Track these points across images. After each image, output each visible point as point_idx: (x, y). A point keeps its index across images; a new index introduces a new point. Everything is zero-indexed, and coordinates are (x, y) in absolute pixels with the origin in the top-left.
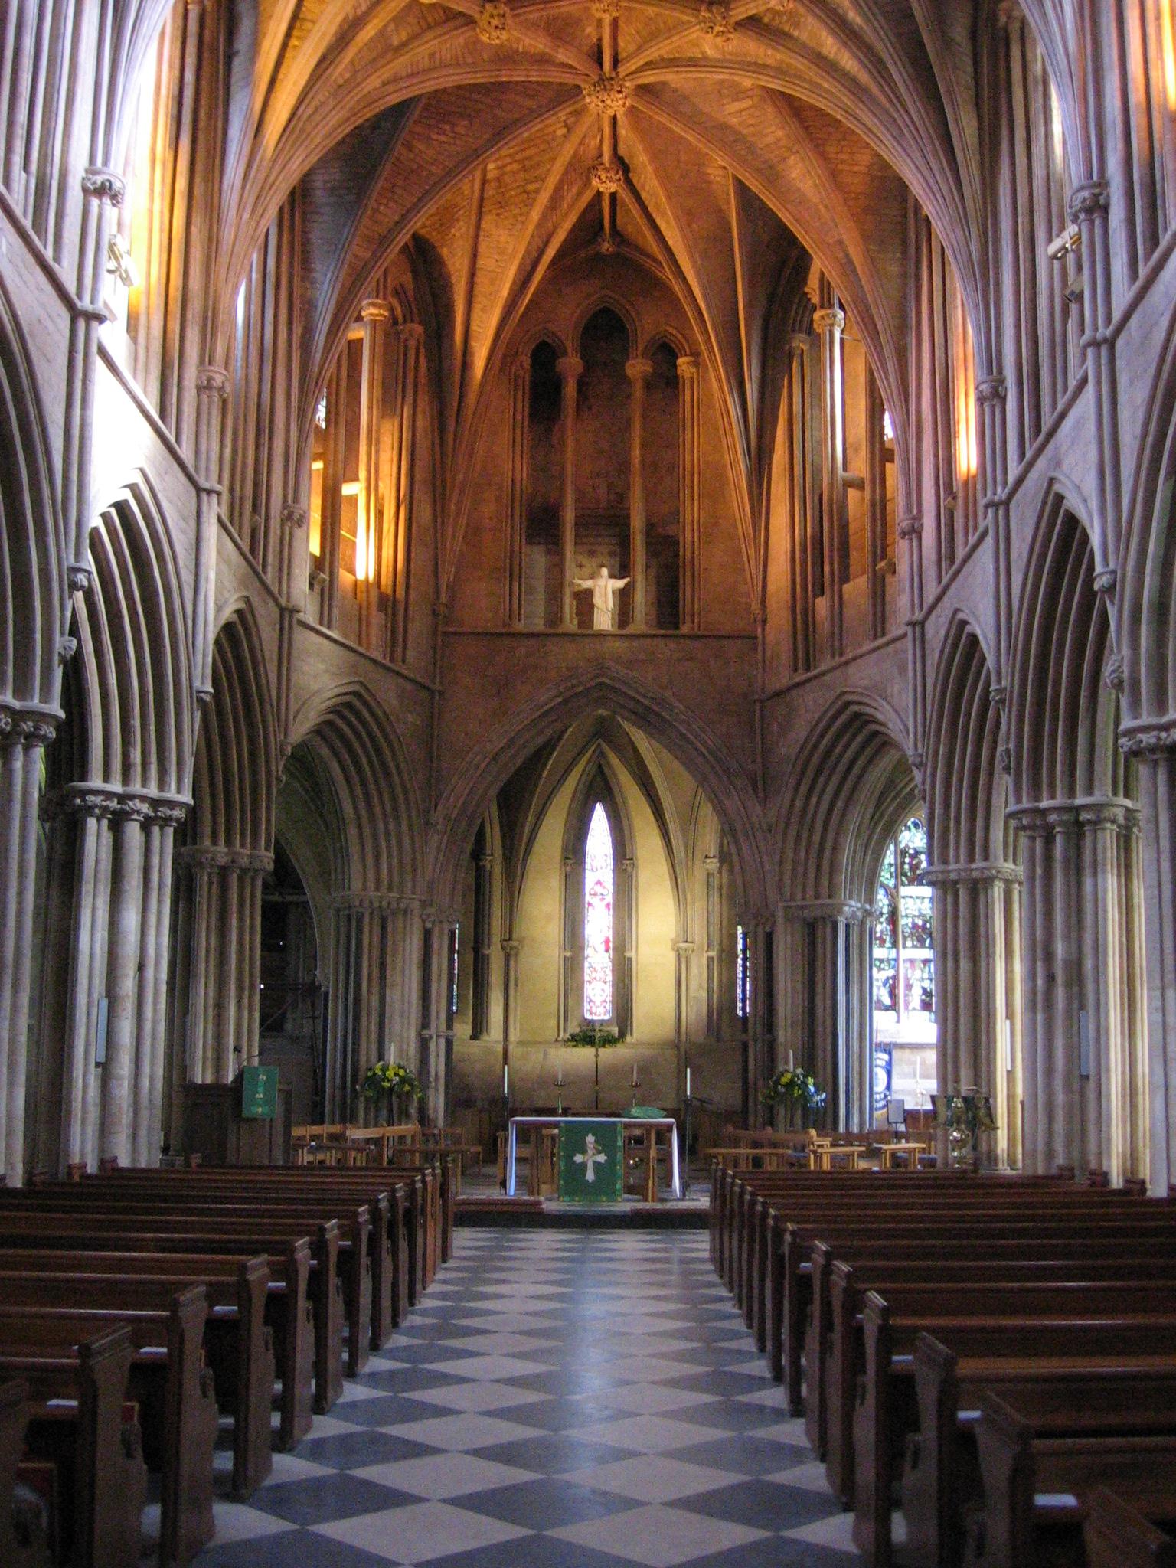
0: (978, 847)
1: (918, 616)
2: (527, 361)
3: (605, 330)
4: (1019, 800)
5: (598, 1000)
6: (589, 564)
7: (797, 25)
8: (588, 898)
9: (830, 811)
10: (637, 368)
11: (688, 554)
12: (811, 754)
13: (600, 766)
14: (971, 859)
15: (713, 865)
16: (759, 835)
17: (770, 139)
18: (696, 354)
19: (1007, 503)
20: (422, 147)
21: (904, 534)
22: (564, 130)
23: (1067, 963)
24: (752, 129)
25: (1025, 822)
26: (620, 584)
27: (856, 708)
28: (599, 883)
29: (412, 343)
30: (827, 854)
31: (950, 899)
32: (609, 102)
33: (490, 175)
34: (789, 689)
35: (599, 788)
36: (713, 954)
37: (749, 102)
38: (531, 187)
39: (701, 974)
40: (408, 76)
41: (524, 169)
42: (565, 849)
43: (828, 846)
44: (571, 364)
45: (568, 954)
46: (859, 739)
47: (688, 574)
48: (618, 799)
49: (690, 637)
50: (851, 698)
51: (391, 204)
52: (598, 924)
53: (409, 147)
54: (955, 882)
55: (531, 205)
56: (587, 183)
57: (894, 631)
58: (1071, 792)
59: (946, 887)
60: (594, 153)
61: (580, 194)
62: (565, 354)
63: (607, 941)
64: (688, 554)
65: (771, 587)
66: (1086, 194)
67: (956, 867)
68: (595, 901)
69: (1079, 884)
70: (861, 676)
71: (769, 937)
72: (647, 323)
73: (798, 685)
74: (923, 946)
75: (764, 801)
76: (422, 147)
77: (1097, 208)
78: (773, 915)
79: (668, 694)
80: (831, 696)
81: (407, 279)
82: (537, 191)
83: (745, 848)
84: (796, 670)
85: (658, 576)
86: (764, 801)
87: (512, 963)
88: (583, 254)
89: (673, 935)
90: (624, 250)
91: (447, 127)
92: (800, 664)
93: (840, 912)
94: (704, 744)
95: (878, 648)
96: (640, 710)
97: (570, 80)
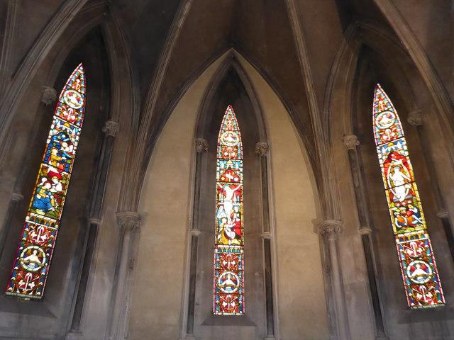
28: (229, 170)
35: (231, 92)
36: (367, 230)
39: (355, 256)
45: (197, 233)
52: (229, 208)
68: (227, 188)
87: (127, 238)
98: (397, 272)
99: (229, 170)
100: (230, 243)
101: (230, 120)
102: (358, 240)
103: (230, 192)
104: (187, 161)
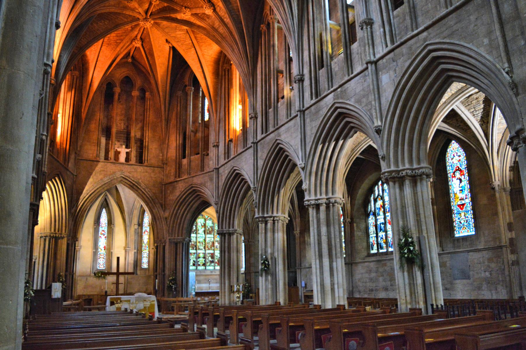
0: (231, 224)
1: (217, 167)
2: (105, 87)
3: (127, 81)
4: (259, 214)
5: (102, 263)
6: (118, 144)
7: (208, 18)
8: (100, 235)
9: (183, 215)
10: (135, 93)
11: (147, 144)
12: (180, 199)
13: (106, 199)
14: (229, 228)
15: (136, 227)
16: (162, 220)
17: (187, 43)
18: (152, 92)
19: (257, 143)
20: (95, 25)
21: (214, 146)
23: (271, 254)
25: (260, 219)
26: (128, 150)
27: (195, 188)
28: (103, 231)
29: (75, 77)
30: (182, 225)
31: (223, 238)
34: (174, 182)
37: (183, 32)
38: (118, 41)
41: (117, 36)
42: (95, 221)
43: (182, 222)
44: (117, 90)
46: (194, 196)
47: (146, 149)
48: (110, 207)
49: (146, 166)
50: (193, 186)
52: (102, 242)
53: (92, 24)
54: (225, 234)
56: (131, 43)
57: (207, 169)
58: (272, 213)
59: (221, 234)
60: (135, 36)
61: (129, 46)
62: (116, 86)
63: (105, 247)
64: (147, 144)
65: (169, 155)
66: (299, 77)
67: (225, 230)
68: (102, 236)
69: (273, 235)
70: (197, 180)
71: (164, 247)
72: (138, 82)
73: (176, 181)
74: (193, 249)
75: (164, 211)
76: (95, 25)
77: (301, 80)
78: (165, 241)
79: (140, 181)
80: (187, 185)
82: (120, 43)
83: (158, 222)
84: (176, 177)
85: (136, 149)
86: (164, 211)
88: (124, 60)
89: (124, 245)
92: (177, 176)
93: (184, 240)
94: (149, 195)
95: (203, 174)
96: (132, 184)
97: (137, 16)
98: (141, 260)
99: (103, 231)
100: (102, 252)
101: (104, 210)
102: (133, 253)
103: (103, 237)
104: (91, 230)
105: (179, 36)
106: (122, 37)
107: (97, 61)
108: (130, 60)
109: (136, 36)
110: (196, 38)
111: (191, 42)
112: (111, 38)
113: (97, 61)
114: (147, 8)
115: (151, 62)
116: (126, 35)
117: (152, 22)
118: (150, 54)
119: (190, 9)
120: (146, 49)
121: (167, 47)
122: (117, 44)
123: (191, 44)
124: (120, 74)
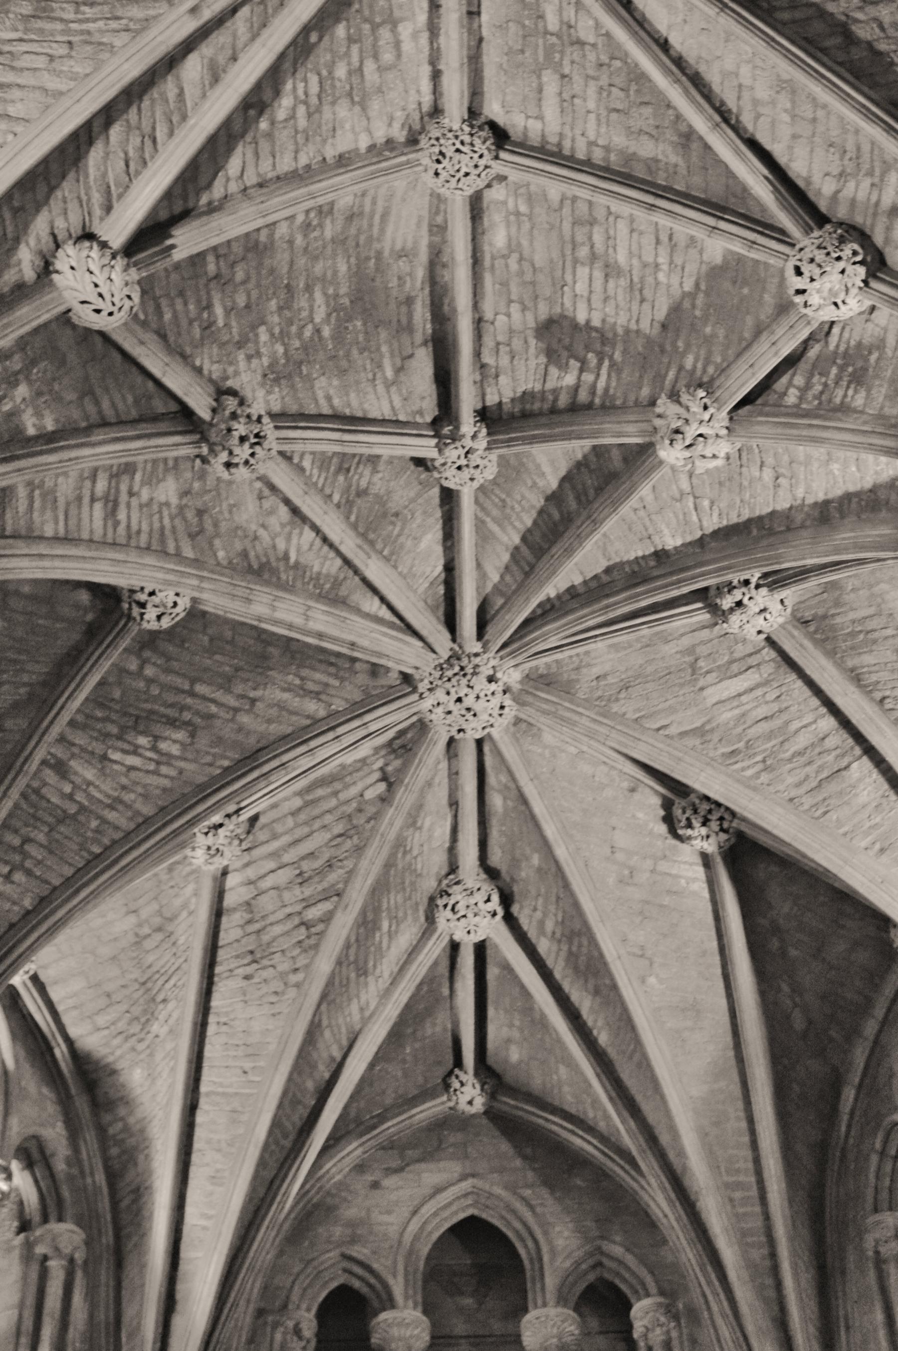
2: (309, 1328)
7: (858, 379)
17: (802, 741)
20: (89, 774)
22: (382, 786)
24: (764, 727)
29: (56, 1266)
32: (469, 701)
33: (230, 900)
37: (752, 678)
40: (56, 539)
41: (303, 879)
51: (18, 877)
53: (60, 768)
55: (316, 947)
56: (430, 919)
60: (438, 861)
62: (389, 1303)
72: (557, 1241)
76: (89, 774)
81: (55, 1135)
82: (327, 919)
90: (507, 1103)
91: (143, 741)
105: (727, 716)
106: (333, 877)
107: (191, 1108)
108: (470, 1095)
109: (453, 868)
110: (856, 677)
111: (828, 723)
112: (267, 903)
113: (191, 1108)
114: (438, 569)
115: (603, 1038)
116: (359, 850)
117: (512, 676)
118: (579, 971)
119: (708, 386)
120: (543, 946)
121: (687, 865)
122: (312, 932)
123: (840, 739)
124: (406, 1212)
